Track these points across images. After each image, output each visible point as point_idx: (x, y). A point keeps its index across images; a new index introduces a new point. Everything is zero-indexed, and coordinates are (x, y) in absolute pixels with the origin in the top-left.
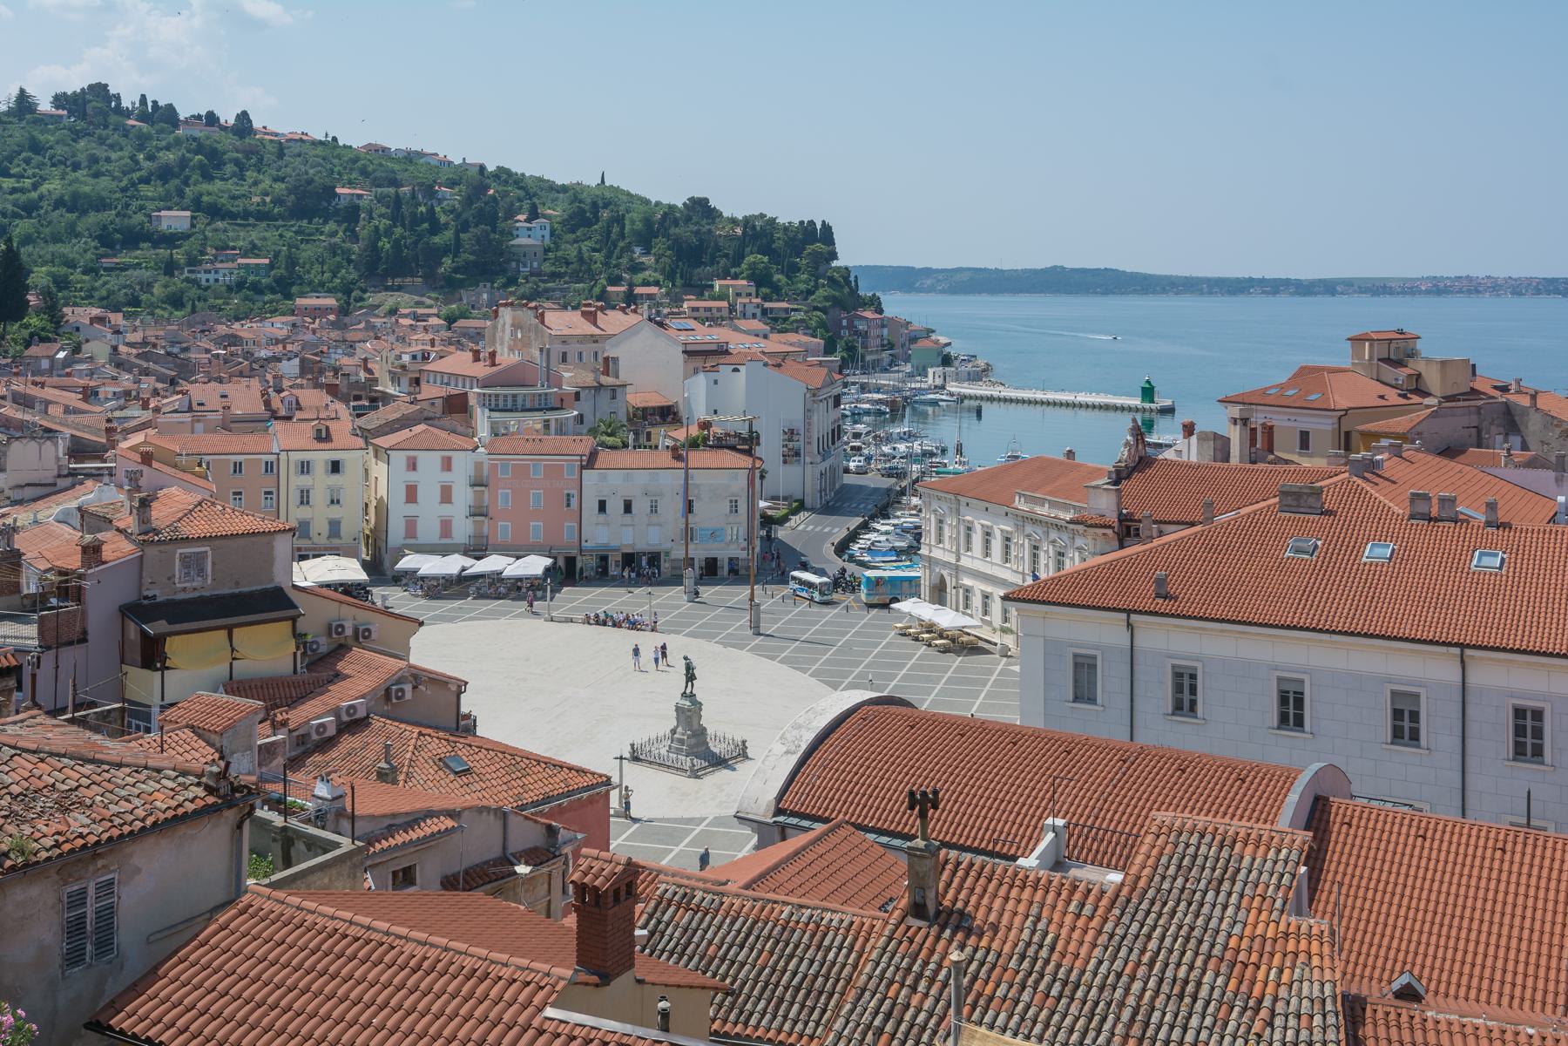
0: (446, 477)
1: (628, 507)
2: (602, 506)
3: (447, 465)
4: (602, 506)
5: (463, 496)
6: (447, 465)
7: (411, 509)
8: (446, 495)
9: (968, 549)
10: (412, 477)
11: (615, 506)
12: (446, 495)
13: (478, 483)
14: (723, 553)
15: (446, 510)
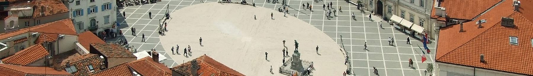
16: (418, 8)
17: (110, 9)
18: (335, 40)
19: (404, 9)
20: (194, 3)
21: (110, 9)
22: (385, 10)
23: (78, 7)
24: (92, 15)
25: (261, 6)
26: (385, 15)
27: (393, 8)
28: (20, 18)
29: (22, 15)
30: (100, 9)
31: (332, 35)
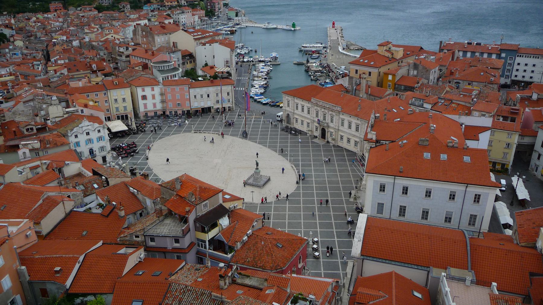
0: (153, 93)
1: (202, 96)
2: (195, 96)
3: (153, 90)
4: (195, 96)
5: (158, 98)
6: (153, 90)
7: (145, 102)
8: (154, 97)
9: (297, 109)
10: (144, 94)
11: (198, 97)
12: (154, 97)
13: (162, 94)
14: (227, 105)
15: (154, 101)
16: (354, 133)
17: (104, 140)
18: (287, 159)
19: (342, 134)
20: (173, 134)
21: (104, 140)
22: (328, 135)
23: (77, 140)
24: (90, 146)
25: (228, 134)
26: (328, 139)
27: (333, 134)
28: (30, 150)
29: (31, 148)
30: (95, 141)
31: (285, 156)
